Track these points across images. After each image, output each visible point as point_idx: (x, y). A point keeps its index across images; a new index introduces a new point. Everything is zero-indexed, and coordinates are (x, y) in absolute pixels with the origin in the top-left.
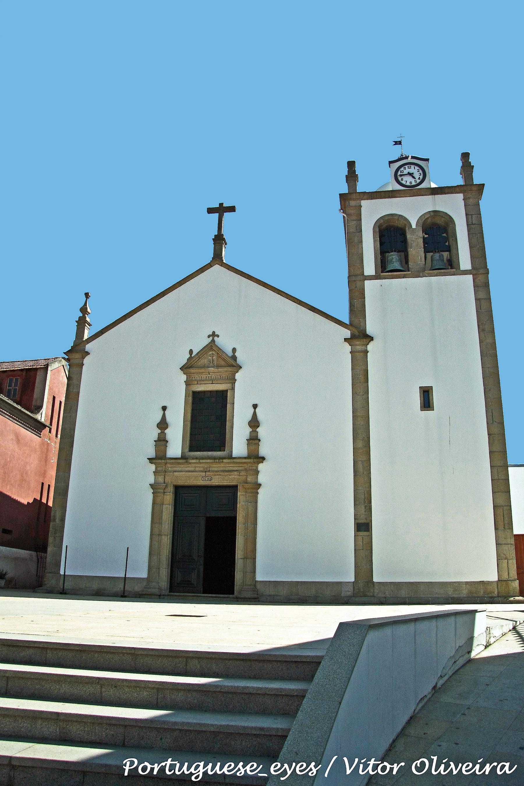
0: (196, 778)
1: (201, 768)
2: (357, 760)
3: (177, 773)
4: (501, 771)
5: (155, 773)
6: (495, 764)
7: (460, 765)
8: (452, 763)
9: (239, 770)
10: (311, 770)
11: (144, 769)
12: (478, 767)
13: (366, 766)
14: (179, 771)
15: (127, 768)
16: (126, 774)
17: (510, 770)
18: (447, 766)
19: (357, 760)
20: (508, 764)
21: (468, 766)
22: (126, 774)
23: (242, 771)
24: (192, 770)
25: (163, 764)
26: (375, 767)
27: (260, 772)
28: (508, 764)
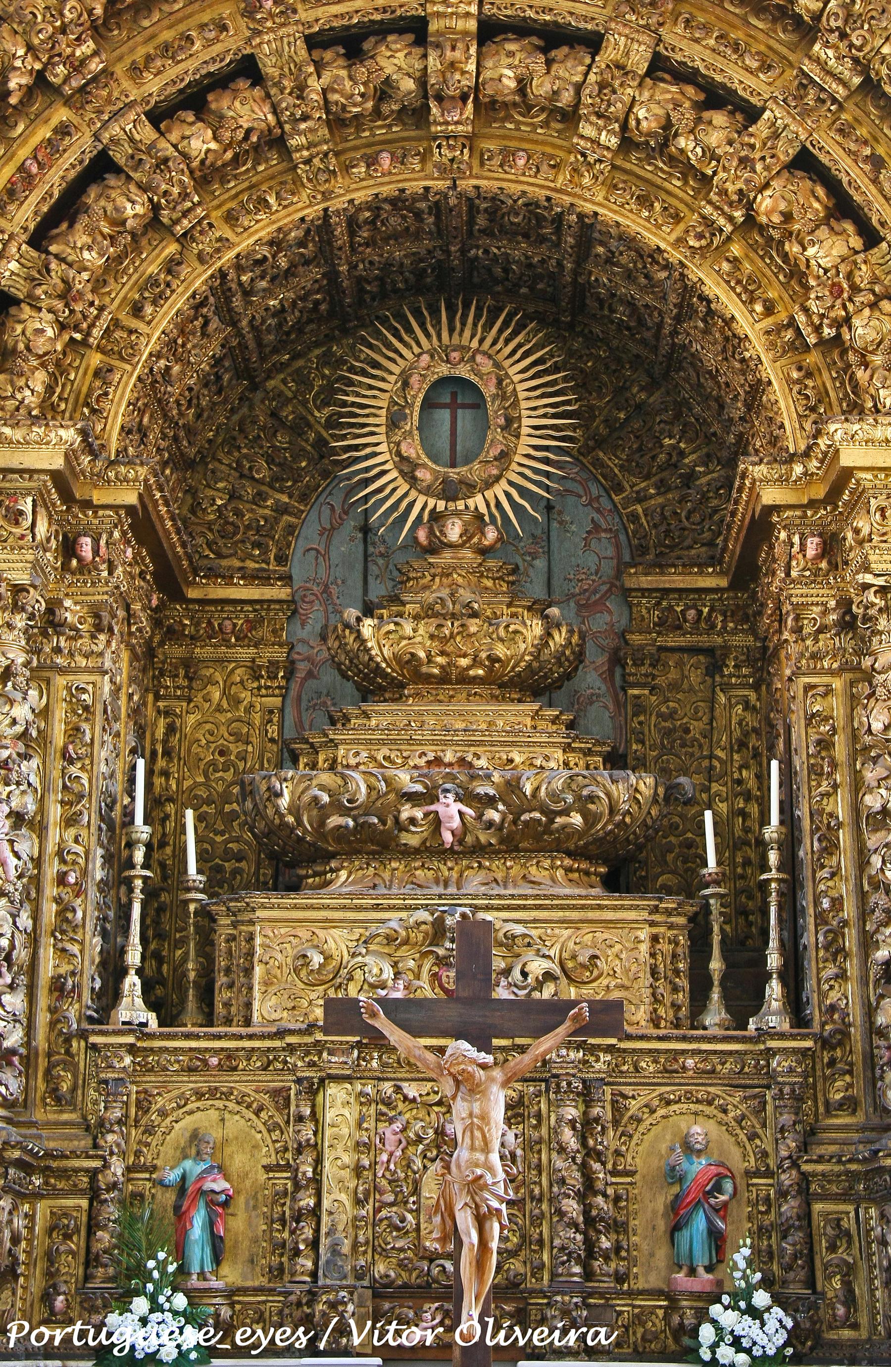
0: (120, 1351)
3: (91, 1343)
5: (57, 1343)
6: (584, 1329)
8: (517, 1329)
10: (298, 1338)
11: (40, 1337)
12: (557, 1334)
13: (383, 1334)
20: (603, 1330)
22: (11, 1345)
26: (398, 1333)
27: (219, 1342)
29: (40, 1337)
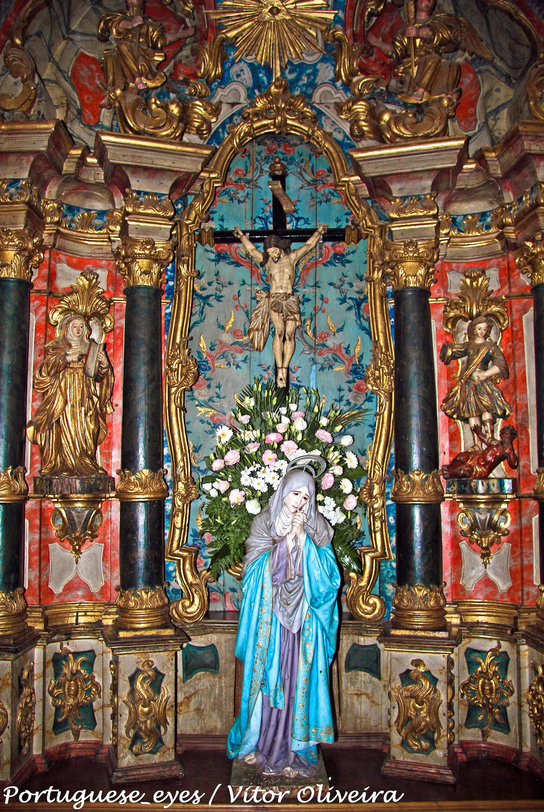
0: (78, 806)
1: (83, 797)
4: (388, 799)
6: (382, 792)
7: (346, 793)
8: (338, 791)
9: (121, 798)
10: (195, 798)
11: (25, 797)
12: (364, 795)
14: (61, 799)
16: (7, 802)
17: (396, 798)
18: (333, 794)
19: (241, 788)
20: (394, 793)
21: (354, 794)
22: (7, 802)
23: (125, 799)
24: (74, 798)
26: (259, 795)
27: (143, 800)
28: (395, 792)
29: (25, 797)
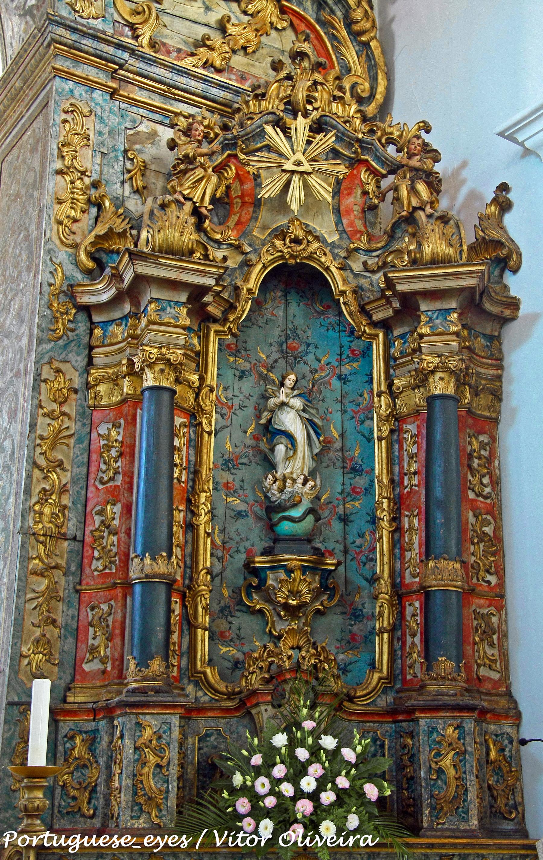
1: (78, 842)
2: (226, 833)
6: (358, 836)
8: (317, 836)
10: (183, 842)
12: (342, 839)
13: (235, 838)
15: (7, 840)
19: (226, 833)
20: (370, 837)
23: (117, 843)
24: (69, 842)
25: (42, 837)
29: (24, 840)
